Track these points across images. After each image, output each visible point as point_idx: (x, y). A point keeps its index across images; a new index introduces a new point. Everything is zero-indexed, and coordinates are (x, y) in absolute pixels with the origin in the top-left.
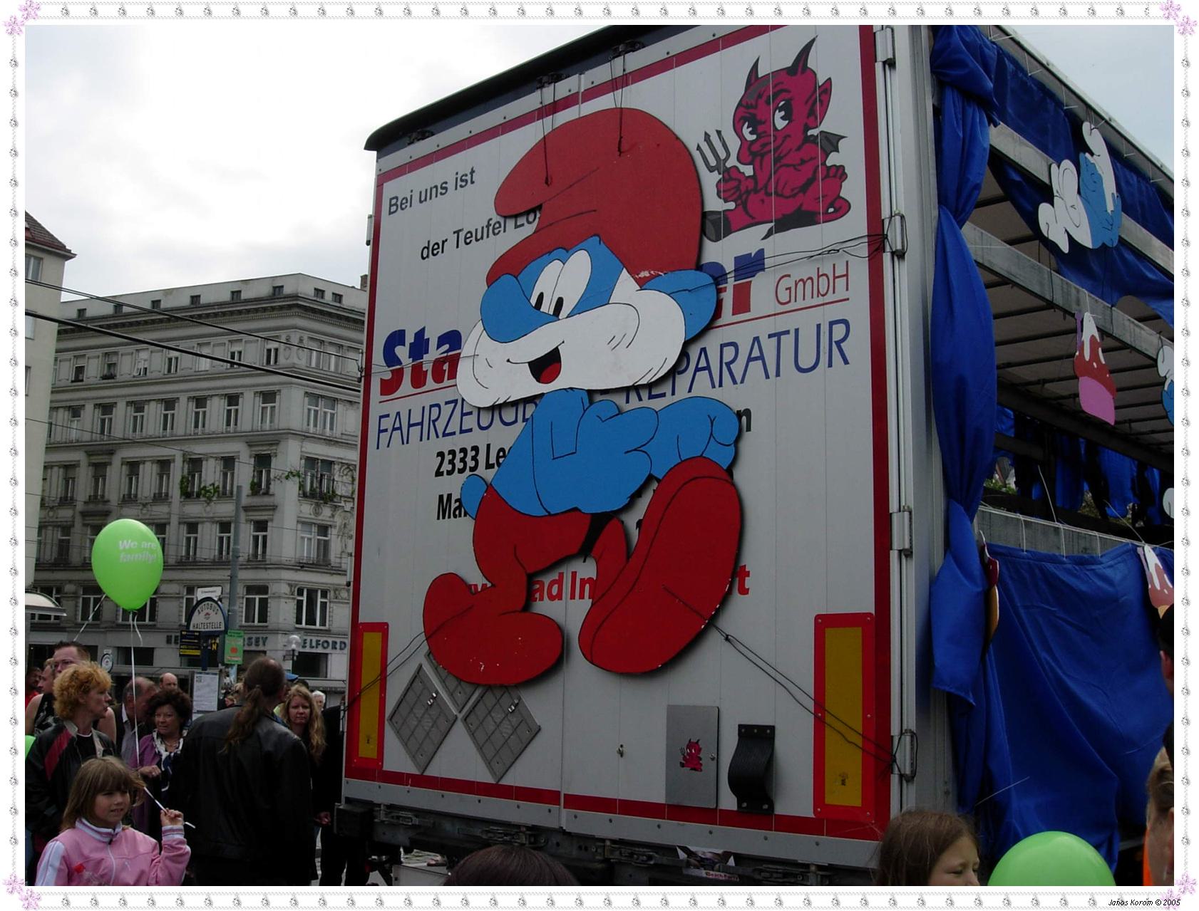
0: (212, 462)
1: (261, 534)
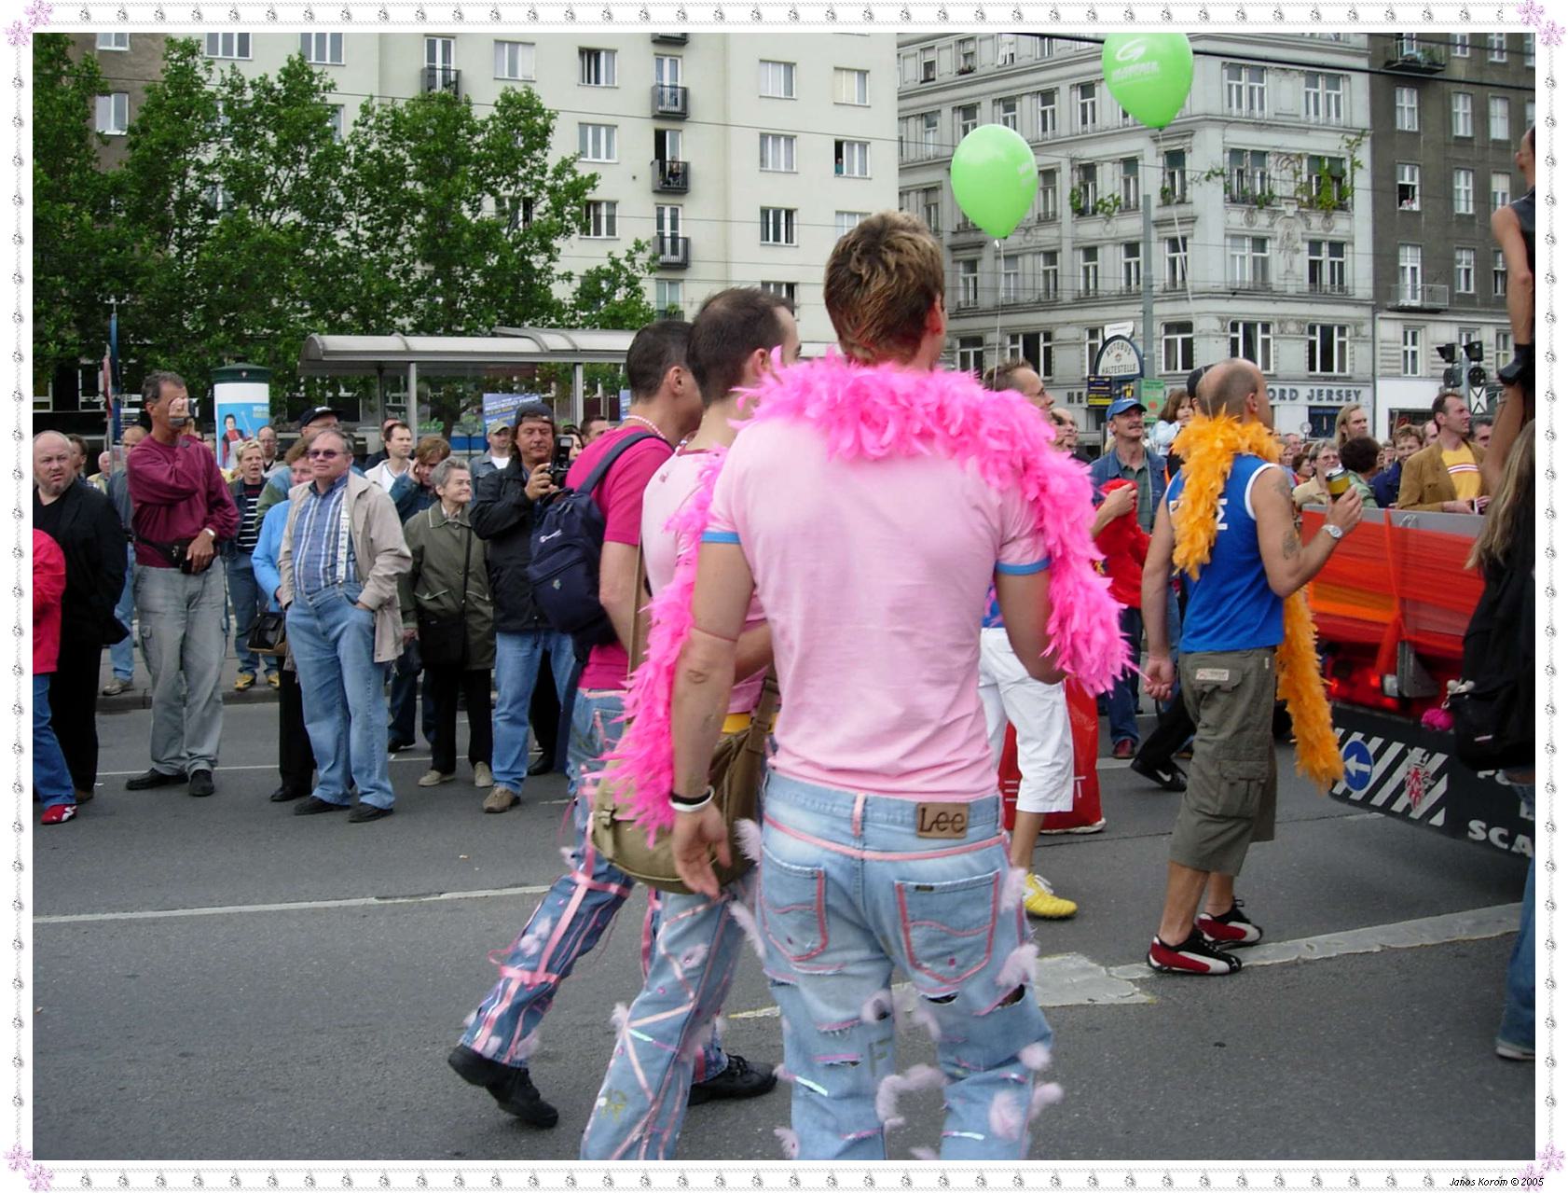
0: (1108, 166)
1: (1133, 260)
